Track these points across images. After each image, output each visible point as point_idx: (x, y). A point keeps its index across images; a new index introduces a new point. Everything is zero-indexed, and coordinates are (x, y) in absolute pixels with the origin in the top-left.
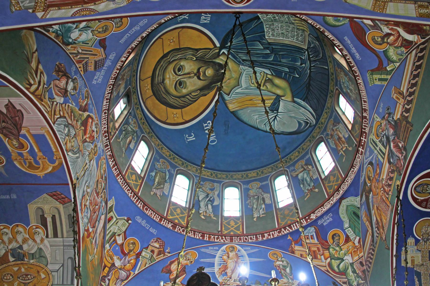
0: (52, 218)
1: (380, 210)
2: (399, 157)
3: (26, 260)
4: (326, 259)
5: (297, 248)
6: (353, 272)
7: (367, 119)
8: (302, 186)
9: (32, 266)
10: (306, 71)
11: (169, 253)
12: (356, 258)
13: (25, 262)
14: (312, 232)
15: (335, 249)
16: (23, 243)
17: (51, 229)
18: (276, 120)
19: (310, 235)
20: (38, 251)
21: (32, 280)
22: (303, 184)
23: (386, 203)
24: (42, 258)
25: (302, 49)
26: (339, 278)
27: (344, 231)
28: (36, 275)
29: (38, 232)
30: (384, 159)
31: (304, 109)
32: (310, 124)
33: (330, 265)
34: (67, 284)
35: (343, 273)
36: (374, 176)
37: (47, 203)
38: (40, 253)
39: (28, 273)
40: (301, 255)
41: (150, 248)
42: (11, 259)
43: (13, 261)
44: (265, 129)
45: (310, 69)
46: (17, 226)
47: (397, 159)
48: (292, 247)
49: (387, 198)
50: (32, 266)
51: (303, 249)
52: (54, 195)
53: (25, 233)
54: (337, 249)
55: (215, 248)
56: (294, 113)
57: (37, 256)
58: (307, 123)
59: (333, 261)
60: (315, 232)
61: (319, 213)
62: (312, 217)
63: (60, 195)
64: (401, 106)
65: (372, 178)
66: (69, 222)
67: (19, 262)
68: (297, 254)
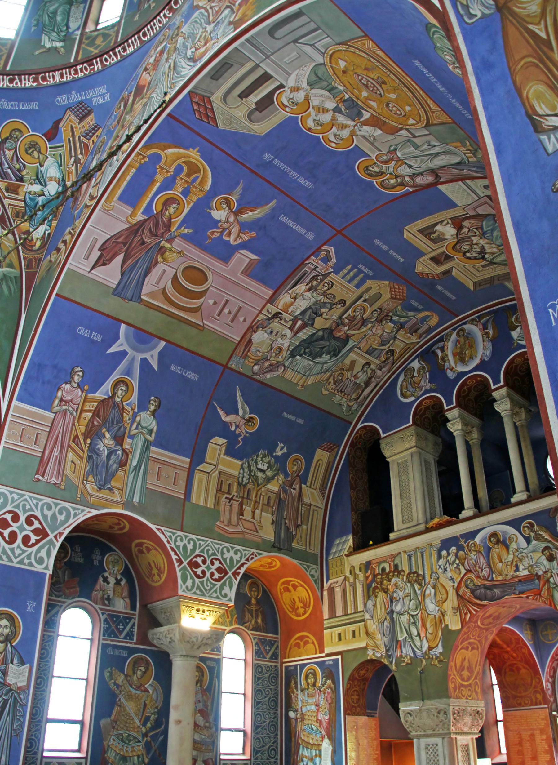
0: (246, 97)
9: (348, 85)
16: (327, 111)
17: (265, 88)
24: (320, 76)
29: (288, 102)
37: (231, 117)
38: (316, 83)
42: (366, 115)
46: (309, 130)
50: (348, 85)
52: (208, 117)
53: (309, 115)
63: (199, 111)
66: (225, 72)
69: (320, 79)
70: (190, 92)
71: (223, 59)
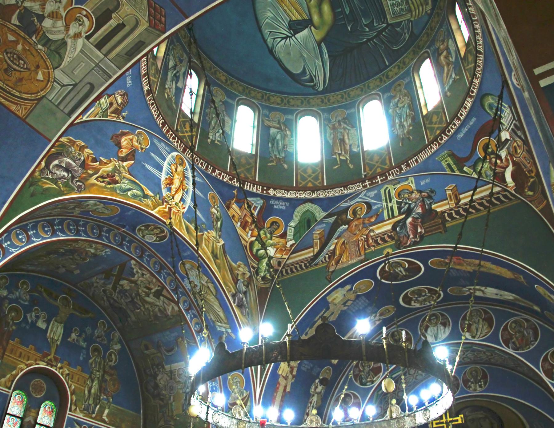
0: (119, 25)
1: (346, 248)
2: (409, 236)
3: (34, 38)
4: (252, 236)
5: (234, 206)
6: (267, 264)
7: (401, 172)
8: (270, 145)
9: (34, 52)
10: (362, 35)
11: (123, 118)
12: (279, 256)
13: (30, 40)
14: (258, 204)
15: (265, 234)
16: (49, 16)
18: (284, 40)
19: (254, 204)
20: (59, 43)
21: (22, 70)
22: (273, 145)
23: (359, 249)
24: (57, 56)
25: (385, 17)
26: (252, 260)
27: (286, 226)
28: (33, 68)
29: (83, 22)
30: (389, 219)
31: (321, 64)
32: (315, 85)
33: (252, 243)
34: (62, 111)
35: (259, 259)
36: (364, 218)
37: (134, 5)
39: (23, 57)
40: (233, 216)
41: (112, 98)
43: (14, 25)
44: (266, 37)
45: (369, 40)
47: (405, 235)
48: (231, 202)
49: (365, 249)
50: (34, 52)
51: (239, 212)
52: (155, 9)
54: (269, 235)
55: (167, 148)
56: (307, 55)
57: (53, 48)
58: (312, 81)
59: (257, 242)
60: (261, 207)
61: (280, 193)
62: (269, 191)
63: (161, 15)
64: (447, 207)
65: (358, 216)
66: (132, 48)
67: (22, 34)
68: (231, 213)
69: (56, 52)
70: (164, 33)
71: (131, 60)
